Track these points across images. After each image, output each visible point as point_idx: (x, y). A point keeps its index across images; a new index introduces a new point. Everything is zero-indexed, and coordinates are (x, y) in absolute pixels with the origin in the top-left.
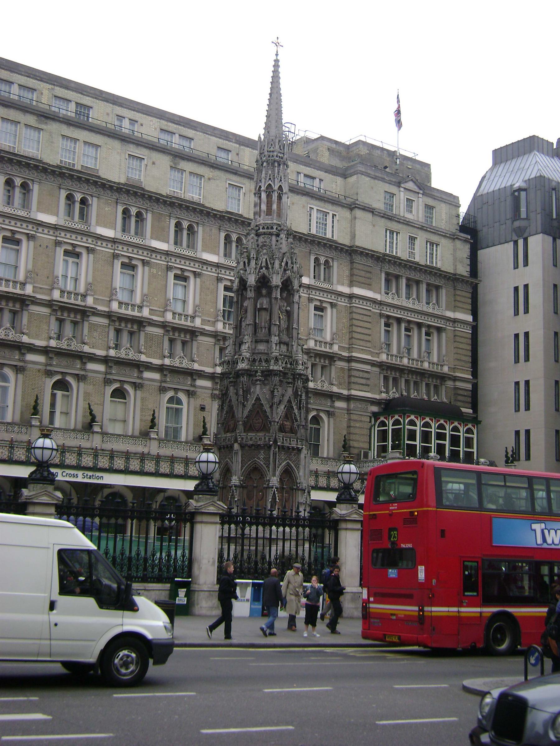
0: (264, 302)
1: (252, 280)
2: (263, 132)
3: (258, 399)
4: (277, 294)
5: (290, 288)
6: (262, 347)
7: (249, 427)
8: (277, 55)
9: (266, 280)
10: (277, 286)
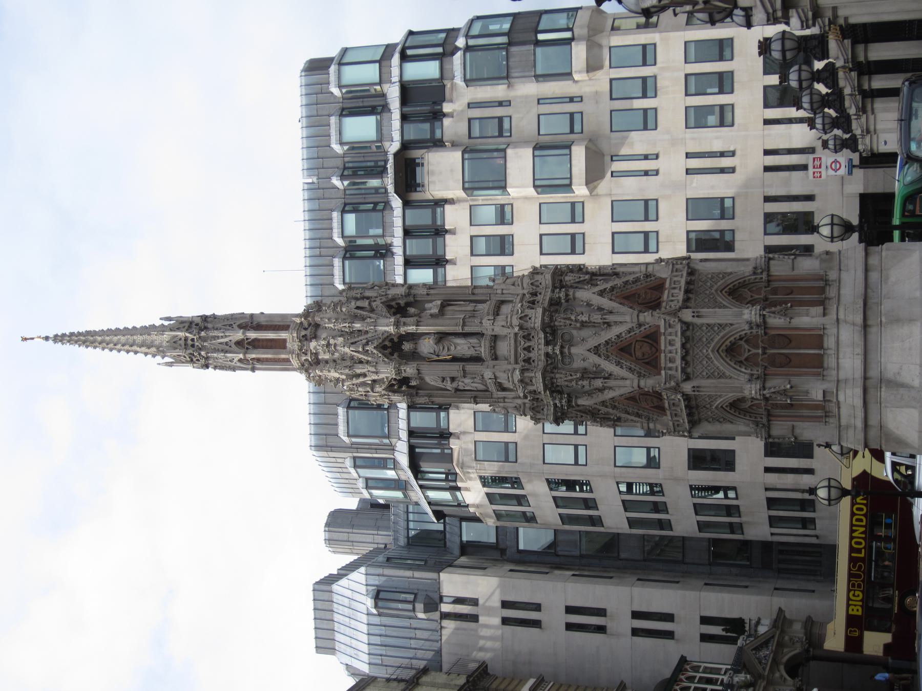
0: (427, 346)
1: (387, 372)
2: (158, 359)
3: (596, 350)
5: (402, 302)
6: (504, 348)
7: (651, 364)
9: (387, 343)
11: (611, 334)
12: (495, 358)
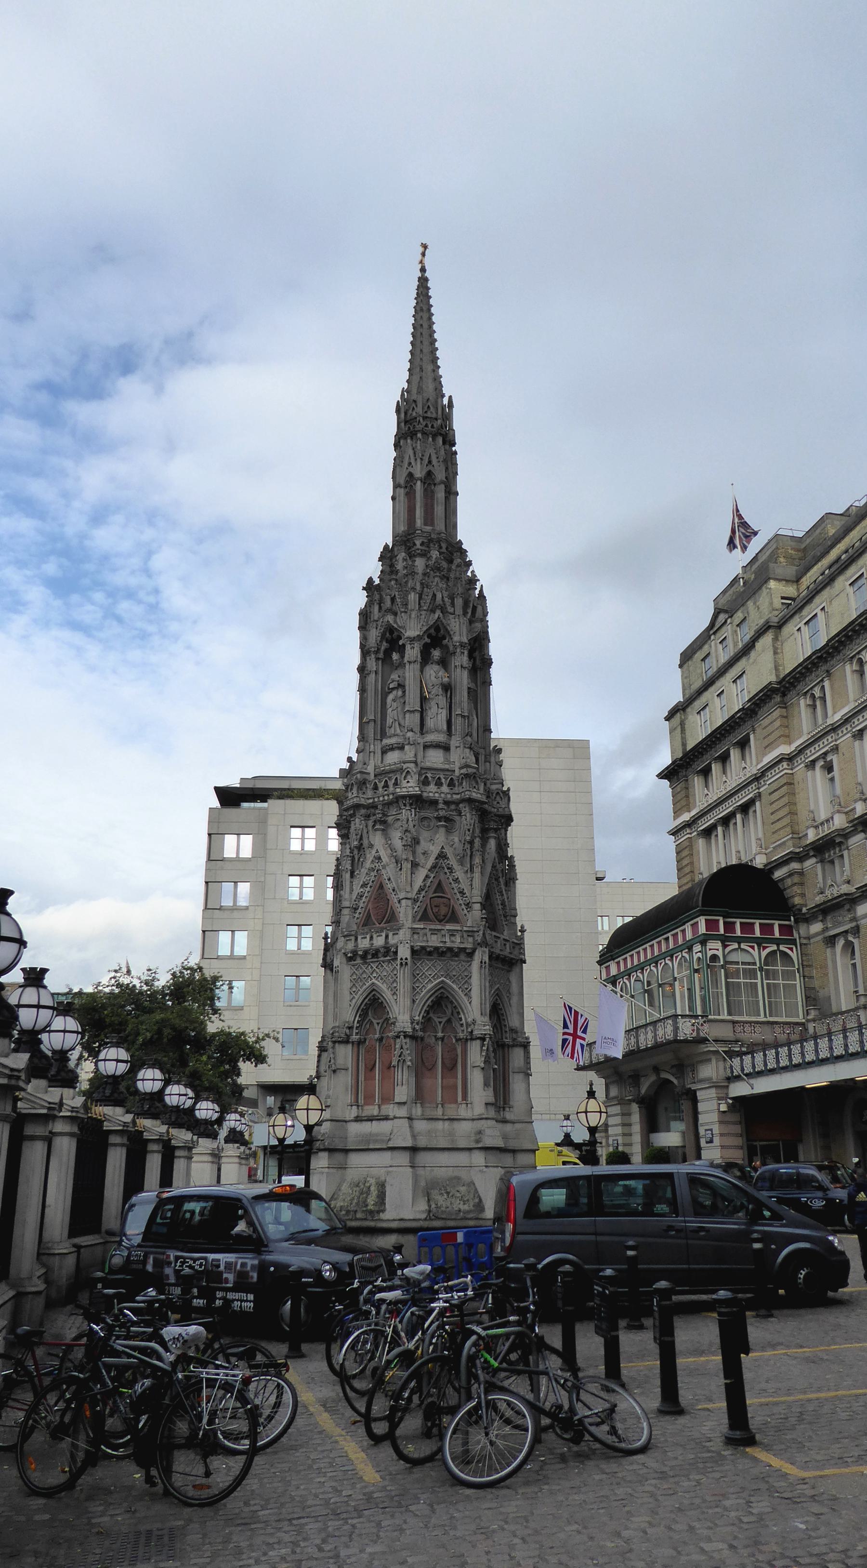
0: (434, 673)
4: (462, 659)
5: (477, 654)
6: (435, 758)
8: (423, 270)
10: (462, 645)
11: (459, 873)
12: (426, 747)
